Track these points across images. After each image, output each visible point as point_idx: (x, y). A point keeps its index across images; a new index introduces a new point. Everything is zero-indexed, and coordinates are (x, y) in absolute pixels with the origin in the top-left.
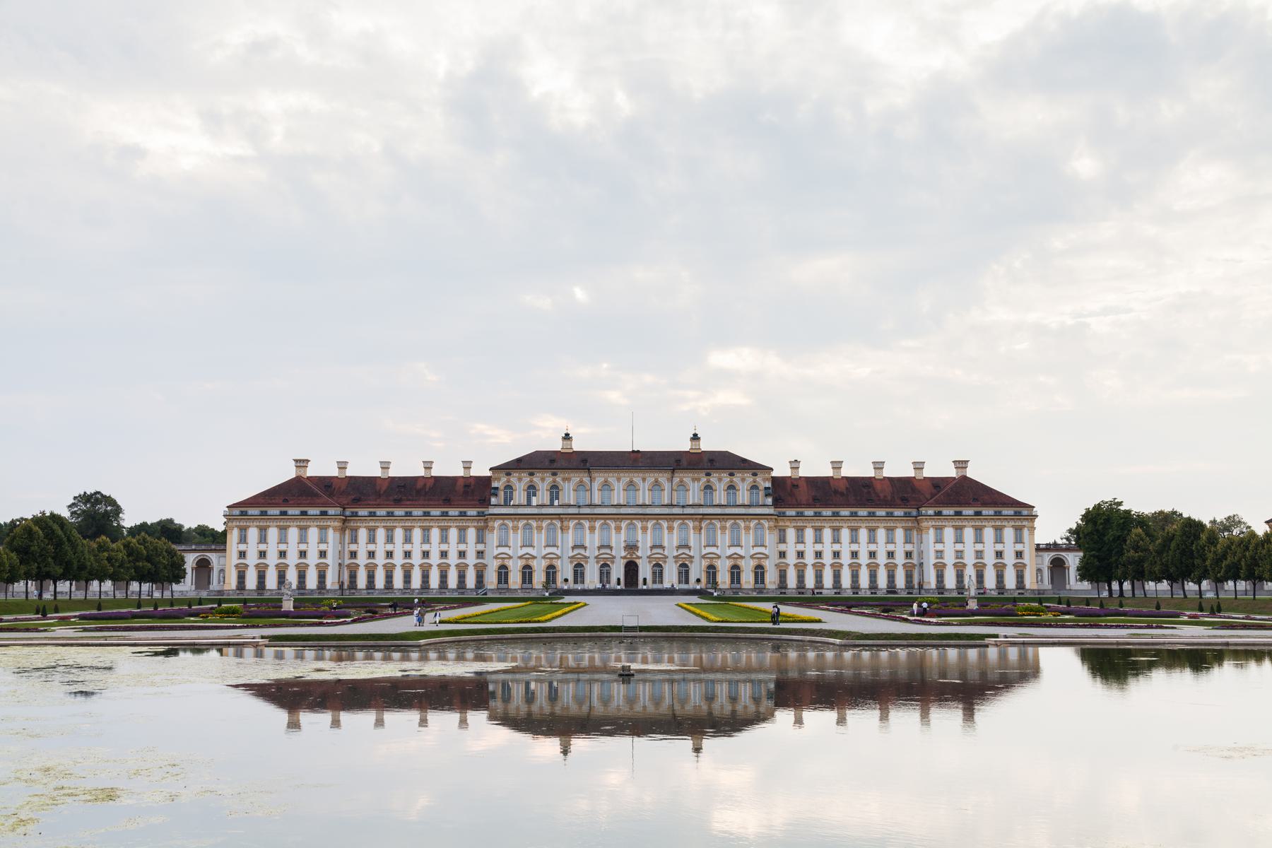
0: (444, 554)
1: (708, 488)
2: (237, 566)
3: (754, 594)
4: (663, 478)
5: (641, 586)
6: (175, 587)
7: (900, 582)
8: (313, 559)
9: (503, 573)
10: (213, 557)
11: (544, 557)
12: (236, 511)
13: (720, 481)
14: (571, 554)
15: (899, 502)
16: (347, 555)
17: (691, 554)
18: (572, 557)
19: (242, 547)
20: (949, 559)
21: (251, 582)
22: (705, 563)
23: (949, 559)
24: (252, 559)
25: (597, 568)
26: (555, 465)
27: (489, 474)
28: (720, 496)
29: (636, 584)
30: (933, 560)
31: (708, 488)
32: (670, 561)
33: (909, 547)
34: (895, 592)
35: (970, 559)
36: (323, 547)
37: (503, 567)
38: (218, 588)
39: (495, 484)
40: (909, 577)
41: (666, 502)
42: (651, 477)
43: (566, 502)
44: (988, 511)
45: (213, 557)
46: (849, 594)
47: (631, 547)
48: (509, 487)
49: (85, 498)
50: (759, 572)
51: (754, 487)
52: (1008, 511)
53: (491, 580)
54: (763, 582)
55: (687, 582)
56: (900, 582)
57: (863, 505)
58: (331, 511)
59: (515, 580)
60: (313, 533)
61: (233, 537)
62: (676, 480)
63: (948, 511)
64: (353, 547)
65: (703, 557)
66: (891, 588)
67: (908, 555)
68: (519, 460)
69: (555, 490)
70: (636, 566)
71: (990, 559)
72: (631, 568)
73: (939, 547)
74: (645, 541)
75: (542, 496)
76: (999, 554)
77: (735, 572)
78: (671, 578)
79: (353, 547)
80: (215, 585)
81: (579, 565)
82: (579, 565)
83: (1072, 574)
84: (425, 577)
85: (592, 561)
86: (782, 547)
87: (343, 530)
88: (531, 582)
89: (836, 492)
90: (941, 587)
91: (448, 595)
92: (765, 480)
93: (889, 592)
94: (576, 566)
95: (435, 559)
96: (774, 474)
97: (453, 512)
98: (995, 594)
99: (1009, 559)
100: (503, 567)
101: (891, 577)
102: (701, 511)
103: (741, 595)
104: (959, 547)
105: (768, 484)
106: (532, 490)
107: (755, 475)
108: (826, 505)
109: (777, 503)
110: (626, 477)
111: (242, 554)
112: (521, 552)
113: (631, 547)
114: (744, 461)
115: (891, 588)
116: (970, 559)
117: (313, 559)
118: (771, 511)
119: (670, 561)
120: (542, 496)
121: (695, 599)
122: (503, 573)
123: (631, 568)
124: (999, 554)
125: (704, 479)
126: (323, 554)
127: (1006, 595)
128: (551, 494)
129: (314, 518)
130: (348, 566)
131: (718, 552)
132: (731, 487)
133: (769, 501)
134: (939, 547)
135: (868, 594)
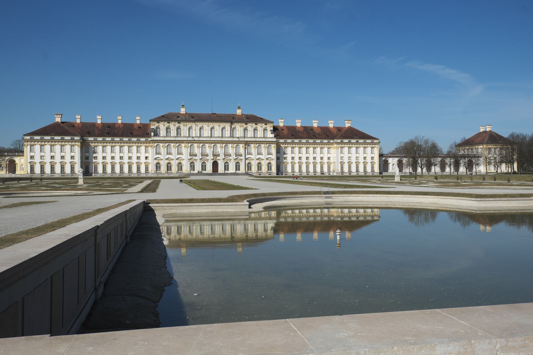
0: (130, 158)
1: (245, 129)
3: (268, 175)
4: (227, 126)
5: (219, 172)
7: (325, 170)
8: (68, 160)
9: (158, 166)
10: (17, 160)
11: (177, 159)
12: (28, 138)
13: (250, 127)
14: (189, 158)
16: (84, 158)
17: (242, 158)
18: (190, 159)
19: (32, 154)
20: (346, 160)
21: (37, 170)
22: (247, 162)
23: (346, 160)
24: (37, 160)
26: (179, 119)
28: (250, 134)
29: (217, 171)
30: (340, 161)
31: (245, 129)
32: (232, 161)
33: (329, 155)
35: (354, 160)
36: (73, 154)
40: (329, 168)
42: (222, 125)
44: (361, 141)
45: (17, 159)
46: (305, 174)
48: (158, 128)
50: (269, 166)
51: (265, 130)
52: (369, 141)
53: (152, 168)
55: (239, 170)
57: (311, 138)
58: (77, 138)
60: (68, 148)
61: (27, 149)
62: (233, 126)
63: (346, 141)
64: (87, 154)
66: (322, 173)
67: (329, 158)
68: (163, 116)
69: (178, 128)
71: (361, 160)
72: (215, 165)
73: (342, 155)
75: (173, 133)
76: (365, 158)
77: (259, 166)
78: (232, 169)
79: (87, 154)
82: (192, 163)
83: (390, 166)
84: (121, 168)
85: (199, 160)
87: (81, 147)
88: (171, 170)
90: (342, 172)
91: (132, 176)
93: (322, 174)
95: (134, 160)
97: (134, 139)
98: (363, 174)
99: (369, 160)
101: (322, 168)
102: (246, 139)
103: (262, 175)
104: (350, 155)
105: (272, 129)
106: (168, 128)
107: (266, 124)
109: (275, 137)
110: (211, 125)
112: (167, 157)
113: (215, 155)
114: (261, 118)
115: (322, 173)
116: (354, 160)
117: (68, 160)
118: (275, 140)
119: (232, 161)
120: (173, 133)
121: (247, 177)
122: (158, 166)
123: (215, 165)
124: (365, 158)
125: (245, 126)
126: (72, 157)
127: (367, 175)
128: (177, 131)
129: (68, 141)
130: (85, 163)
131: (253, 157)
132: (255, 130)
133: (273, 135)
134: (342, 155)
135: (313, 174)
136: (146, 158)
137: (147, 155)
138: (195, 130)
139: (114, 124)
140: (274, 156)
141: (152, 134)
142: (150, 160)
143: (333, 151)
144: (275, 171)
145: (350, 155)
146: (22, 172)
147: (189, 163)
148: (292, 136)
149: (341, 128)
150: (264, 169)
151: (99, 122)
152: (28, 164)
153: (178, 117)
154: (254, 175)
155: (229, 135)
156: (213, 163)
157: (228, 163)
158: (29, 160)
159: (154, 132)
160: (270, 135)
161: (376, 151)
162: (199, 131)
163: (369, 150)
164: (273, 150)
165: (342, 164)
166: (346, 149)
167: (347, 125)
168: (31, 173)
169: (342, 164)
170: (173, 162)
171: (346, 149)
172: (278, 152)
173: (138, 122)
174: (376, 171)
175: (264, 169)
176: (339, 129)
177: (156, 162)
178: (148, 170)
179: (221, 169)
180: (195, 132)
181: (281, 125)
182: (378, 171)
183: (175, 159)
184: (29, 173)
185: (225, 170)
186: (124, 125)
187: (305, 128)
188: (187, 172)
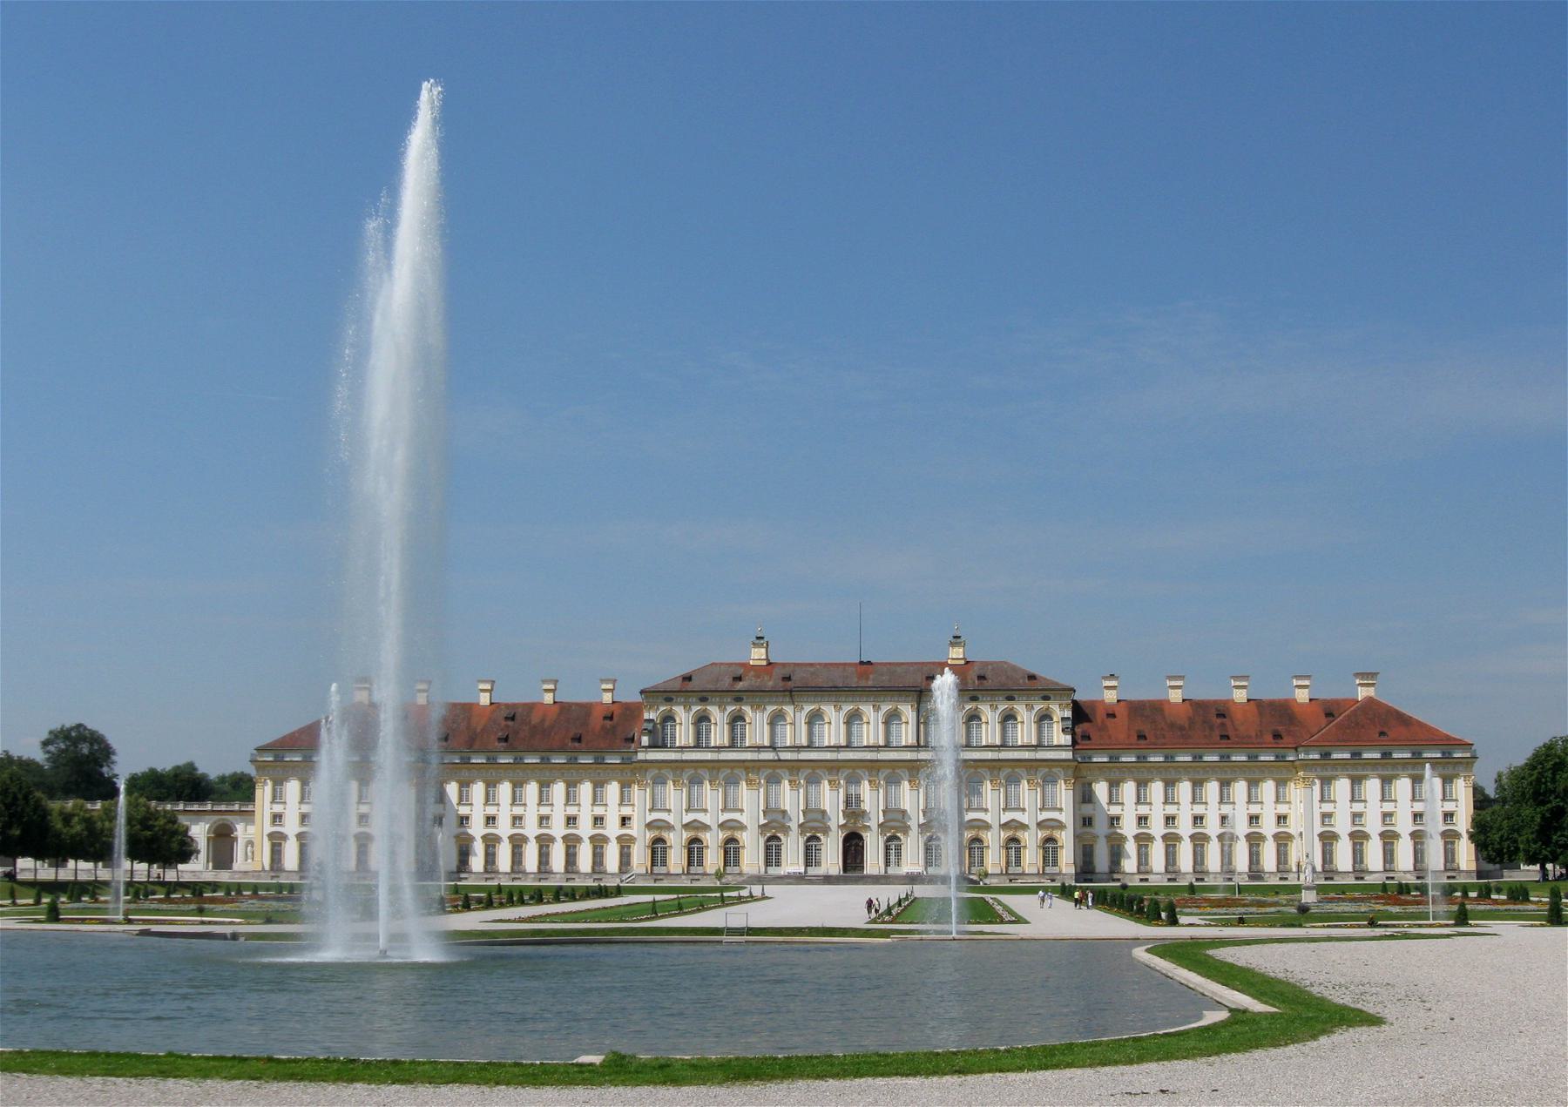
2: (271, 836)
6: (180, 867)
9: (658, 849)
14: (763, 821)
15: (1269, 738)
19: (278, 808)
20: (1343, 826)
22: (968, 835)
23: (1343, 826)
25: (802, 841)
27: (639, 699)
30: (1318, 829)
33: (1282, 809)
34: (1260, 878)
35: (1373, 826)
37: (659, 840)
38: (243, 868)
39: (646, 716)
40: (1282, 857)
41: (911, 740)
43: (759, 742)
47: (853, 810)
49: (63, 734)
51: (1045, 717)
54: (1055, 863)
56: (1269, 861)
57: (1211, 747)
59: (676, 859)
61: (264, 792)
65: (964, 826)
66: (1255, 872)
67: (1281, 819)
68: (687, 678)
70: (861, 838)
72: (853, 847)
73: (1327, 808)
74: (871, 798)
75: (718, 734)
80: (239, 864)
81: (774, 838)
86: (1087, 809)
89: (1172, 726)
90: (1329, 871)
91: (578, 882)
92: (1062, 709)
94: (769, 839)
96: (1077, 697)
100: (659, 840)
103: (1018, 883)
104: (1358, 807)
105: (1068, 714)
106: (702, 719)
108: (1155, 748)
109: (1074, 742)
111: (277, 818)
112: (688, 818)
113: (853, 810)
116: (1373, 826)
120: (718, 734)
122: (658, 849)
123: (853, 847)
131: (987, 817)
133: (1069, 738)
134: (1327, 808)
136: (624, 821)
137: (626, 811)
138: (793, 724)
139: (530, 707)
140: (1066, 817)
141: (645, 740)
142: (635, 829)
143: (1295, 791)
144: (1072, 870)
145: (1358, 807)
146: (250, 866)
147: (762, 841)
148: (1141, 737)
149: (1337, 702)
150: (1031, 859)
151: (484, 700)
152: (266, 839)
153: (739, 679)
154: (993, 882)
155: (911, 740)
156: (847, 840)
157: (980, 841)
158: (269, 829)
159: (650, 732)
160: (1060, 737)
161: (1462, 791)
162: (804, 728)
163: (1433, 783)
164: (1064, 795)
165: (1328, 839)
166: (1342, 786)
167: (1362, 693)
168: (272, 869)
169: (1328, 839)
170: (707, 837)
171: (1342, 786)
172: (1085, 797)
173: (607, 698)
174: (1463, 867)
175: (1031, 859)
176: (1330, 710)
177: (650, 835)
178: (628, 863)
179: (873, 860)
180: (794, 731)
181: (1110, 697)
182: (1473, 867)
183: (714, 827)
184: (267, 868)
185: (768, 863)
186: (563, 708)
187: (1198, 708)
188: (754, 871)
